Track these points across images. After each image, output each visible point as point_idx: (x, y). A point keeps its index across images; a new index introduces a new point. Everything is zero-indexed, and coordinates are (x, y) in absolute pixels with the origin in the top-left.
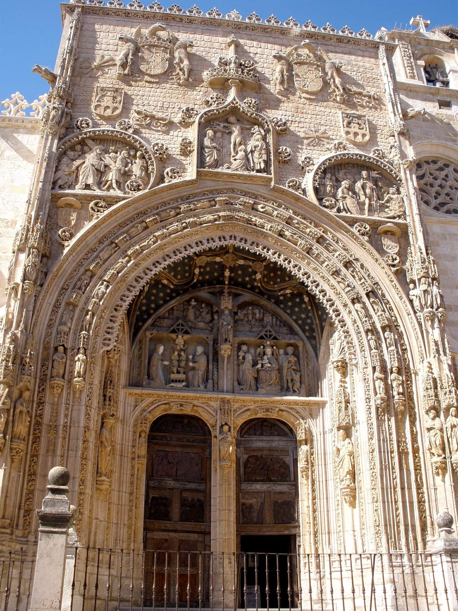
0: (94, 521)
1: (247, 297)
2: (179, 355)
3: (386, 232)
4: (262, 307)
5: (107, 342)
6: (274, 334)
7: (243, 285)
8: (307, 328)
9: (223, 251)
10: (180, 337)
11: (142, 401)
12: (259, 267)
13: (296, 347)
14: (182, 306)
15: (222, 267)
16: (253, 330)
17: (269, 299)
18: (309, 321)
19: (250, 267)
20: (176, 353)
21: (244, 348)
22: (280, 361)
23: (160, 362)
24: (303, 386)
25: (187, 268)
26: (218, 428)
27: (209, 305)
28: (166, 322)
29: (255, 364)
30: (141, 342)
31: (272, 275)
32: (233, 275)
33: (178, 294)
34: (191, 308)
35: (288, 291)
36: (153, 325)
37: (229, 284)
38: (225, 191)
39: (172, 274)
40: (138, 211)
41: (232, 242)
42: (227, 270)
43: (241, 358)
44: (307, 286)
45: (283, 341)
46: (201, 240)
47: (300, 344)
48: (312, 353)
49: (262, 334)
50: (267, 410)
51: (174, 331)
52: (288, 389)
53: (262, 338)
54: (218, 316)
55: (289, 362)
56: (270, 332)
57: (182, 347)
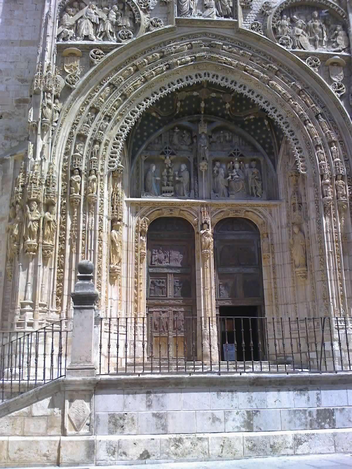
0: (109, 301)
1: (219, 123)
2: (168, 172)
3: (333, 64)
4: (231, 131)
5: (112, 164)
6: (241, 152)
7: (216, 114)
8: (267, 146)
9: (199, 86)
10: (168, 157)
11: (141, 208)
12: (228, 98)
13: (258, 161)
14: (168, 133)
15: (198, 100)
16: (225, 149)
17: (236, 124)
18: (269, 140)
19: (221, 98)
20: (165, 170)
21: (218, 164)
22: (246, 173)
23: (153, 178)
24: (264, 192)
25: (171, 102)
26: (199, 226)
27: (190, 131)
28: (157, 147)
29: (226, 176)
30: (138, 163)
31: (238, 104)
32: (207, 106)
33: (165, 124)
34: (175, 134)
35: (252, 117)
36: (146, 149)
37: (205, 113)
38: (199, 35)
39: (159, 107)
40: (129, 56)
41: (206, 78)
42: (203, 102)
43: (215, 172)
44: (268, 112)
45: (248, 157)
46: (181, 78)
47: (262, 159)
49: (232, 152)
50: (236, 211)
51: (162, 153)
52: (253, 195)
53: (231, 155)
54: (196, 139)
55: (253, 173)
56: (238, 150)
57: (170, 165)
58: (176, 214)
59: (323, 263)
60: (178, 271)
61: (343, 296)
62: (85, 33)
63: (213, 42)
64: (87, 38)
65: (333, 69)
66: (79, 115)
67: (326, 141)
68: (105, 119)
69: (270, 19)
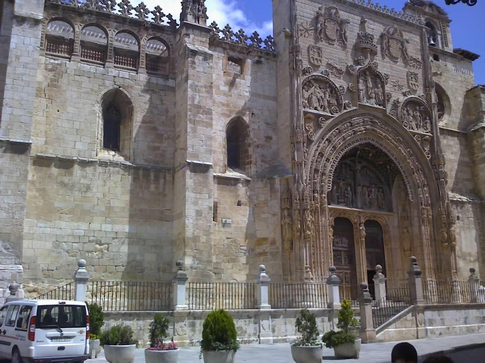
1: (364, 164)
26: (358, 224)
29: (369, 196)
48: (389, 192)
51: (339, 179)
58: (346, 216)
59: (422, 250)
60: (346, 249)
61: (430, 268)
62: (315, 105)
63: (374, 120)
64: (316, 109)
65: (425, 142)
66: (313, 157)
67: (422, 184)
68: (326, 161)
69: (400, 109)
